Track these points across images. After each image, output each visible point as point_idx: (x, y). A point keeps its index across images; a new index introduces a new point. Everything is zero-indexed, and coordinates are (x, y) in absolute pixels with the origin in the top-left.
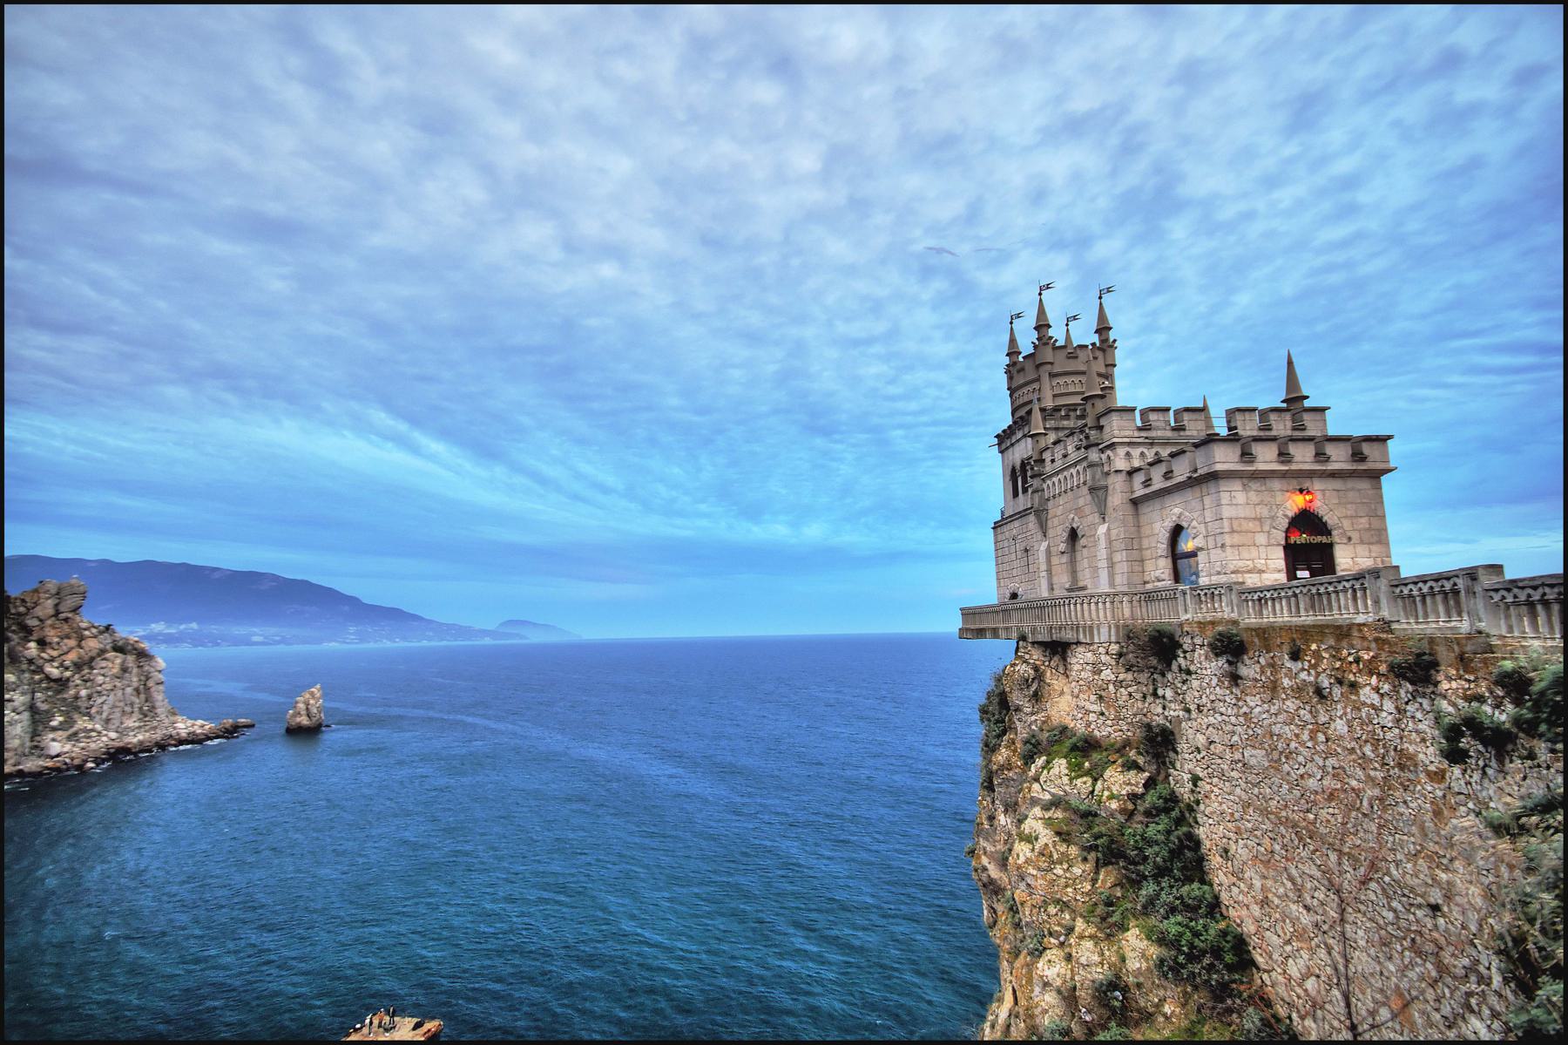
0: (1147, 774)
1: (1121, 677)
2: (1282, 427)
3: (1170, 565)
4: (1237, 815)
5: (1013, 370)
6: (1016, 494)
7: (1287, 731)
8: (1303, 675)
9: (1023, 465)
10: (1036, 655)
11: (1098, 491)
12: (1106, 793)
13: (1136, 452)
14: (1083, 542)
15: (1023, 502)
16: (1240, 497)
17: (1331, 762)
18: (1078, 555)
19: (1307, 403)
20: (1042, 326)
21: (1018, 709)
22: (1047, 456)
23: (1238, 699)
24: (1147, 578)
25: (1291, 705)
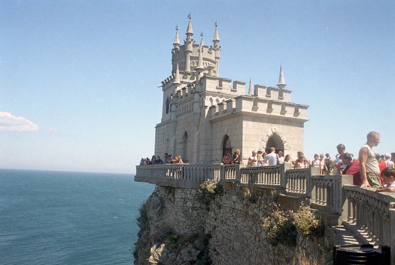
2: (274, 96)
6: (167, 112)
7: (248, 234)
13: (214, 99)
14: (189, 139)
17: (259, 250)
23: (234, 219)
24: (212, 159)
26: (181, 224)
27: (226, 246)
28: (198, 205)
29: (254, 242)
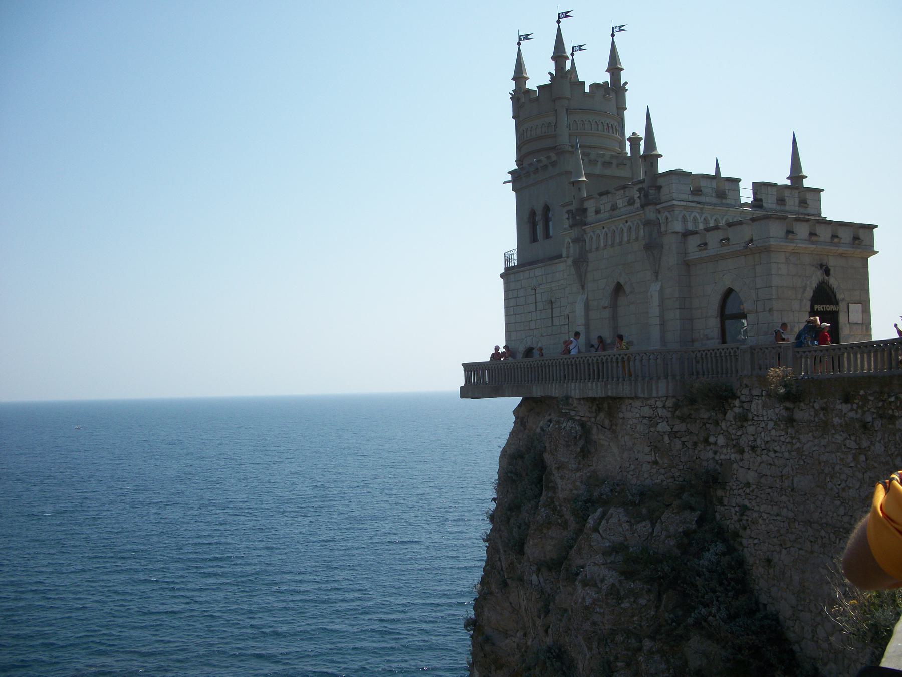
0: (699, 512)
1: (675, 429)
3: (719, 326)
4: (782, 531)
5: (522, 100)
6: (534, 239)
8: (852, 414)
10: (583, 411)
12: (664, 533)
19: (807, 183)
20: (559, 56)
22: (590, 205)
23: (792, 438)
25: (839, 438)
26: (646, 467)
27: (770, 491)
28: (680, 427)
29: (852, 465)
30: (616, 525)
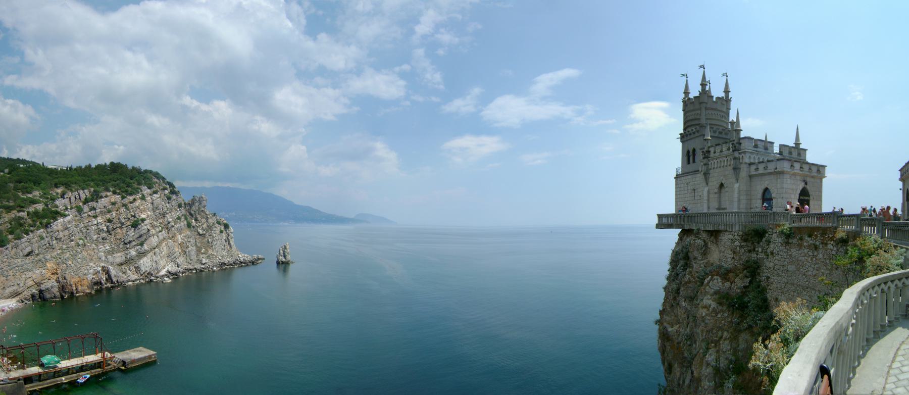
6: (689, 163)
9: (694, 150)
10: (704, 235)
11: (736, 169)
13: (752, 156)
15: (692, 167)
16: (789, 181)
18: (722, 195)
21: (695, 258)
30: (717, 284)
